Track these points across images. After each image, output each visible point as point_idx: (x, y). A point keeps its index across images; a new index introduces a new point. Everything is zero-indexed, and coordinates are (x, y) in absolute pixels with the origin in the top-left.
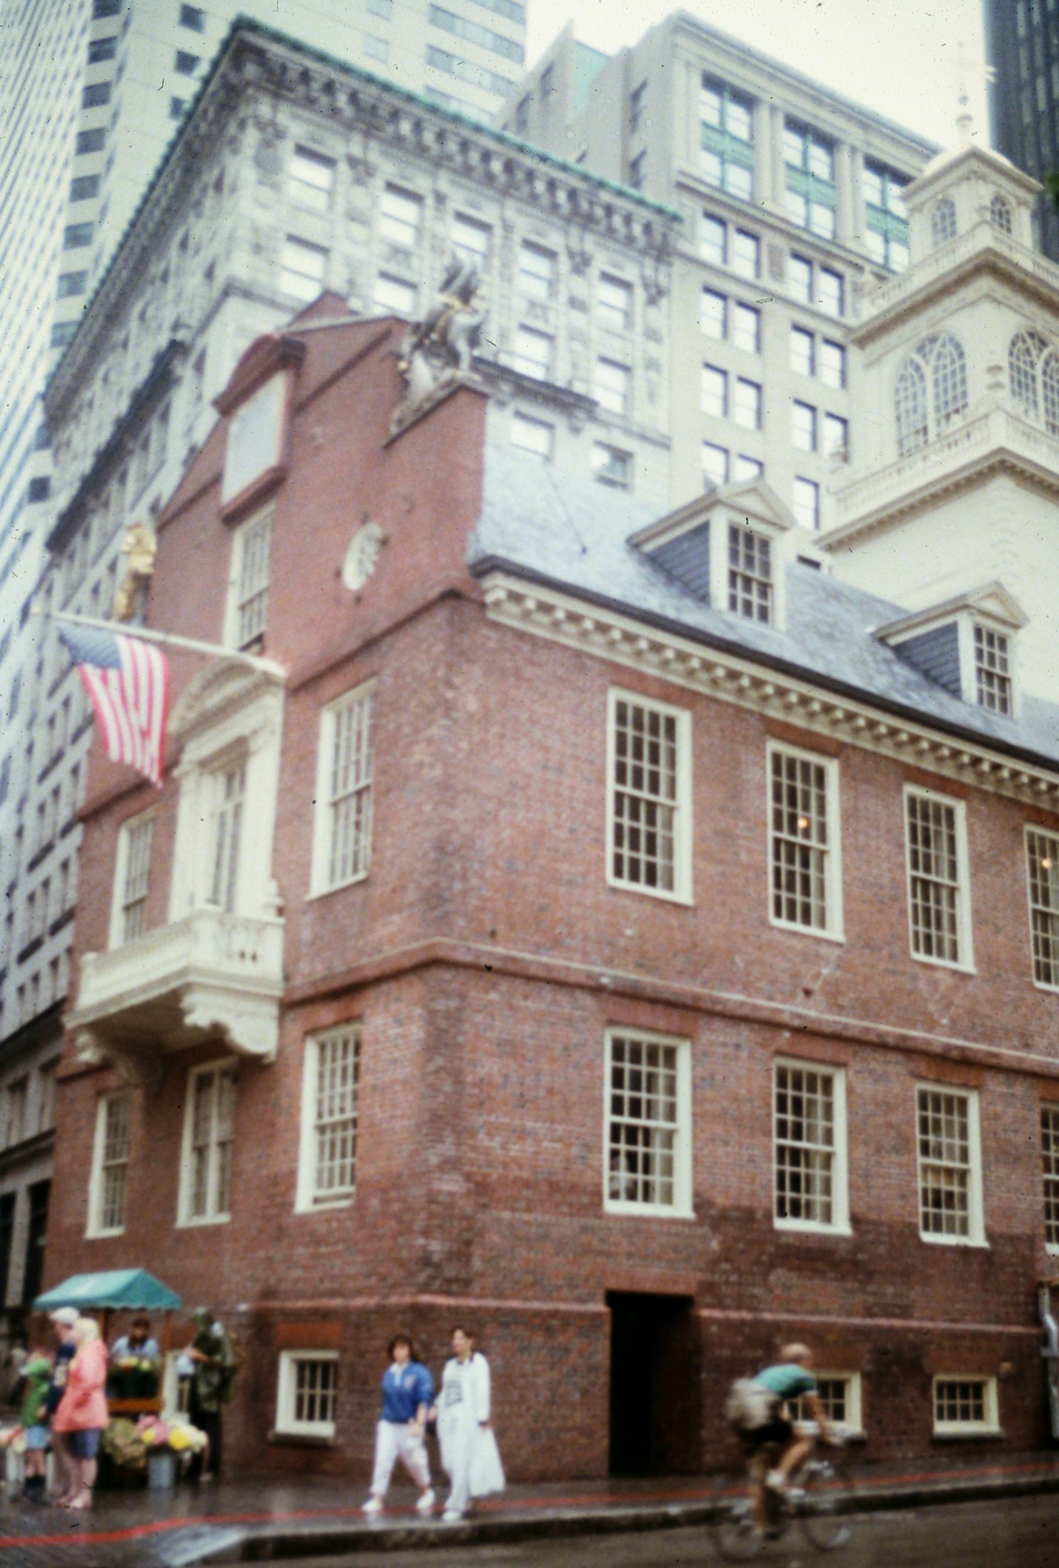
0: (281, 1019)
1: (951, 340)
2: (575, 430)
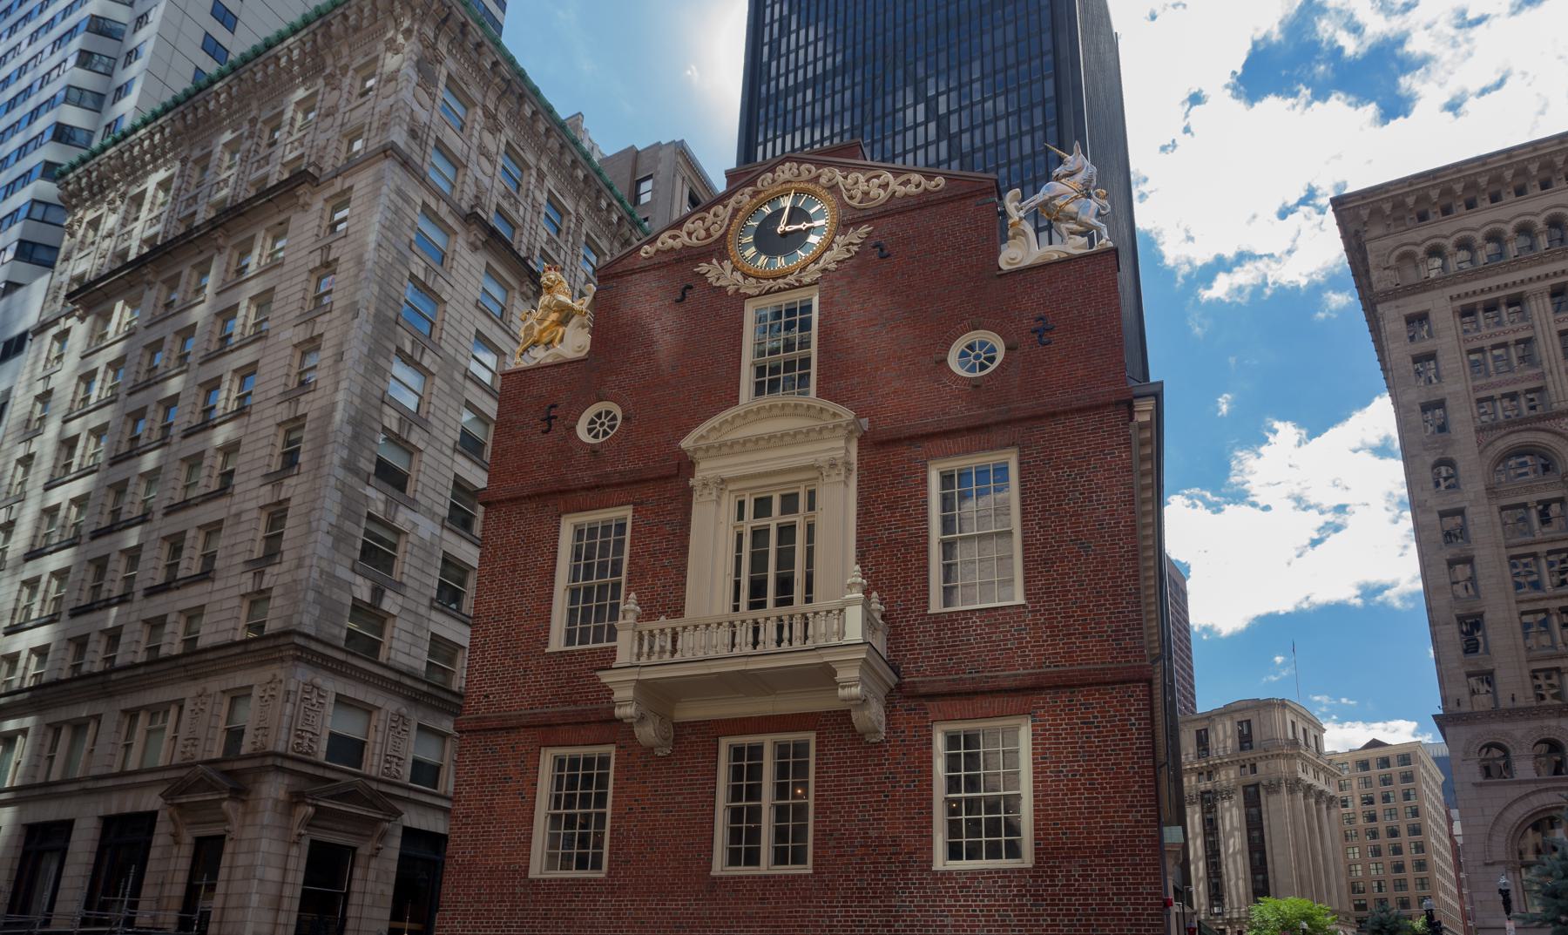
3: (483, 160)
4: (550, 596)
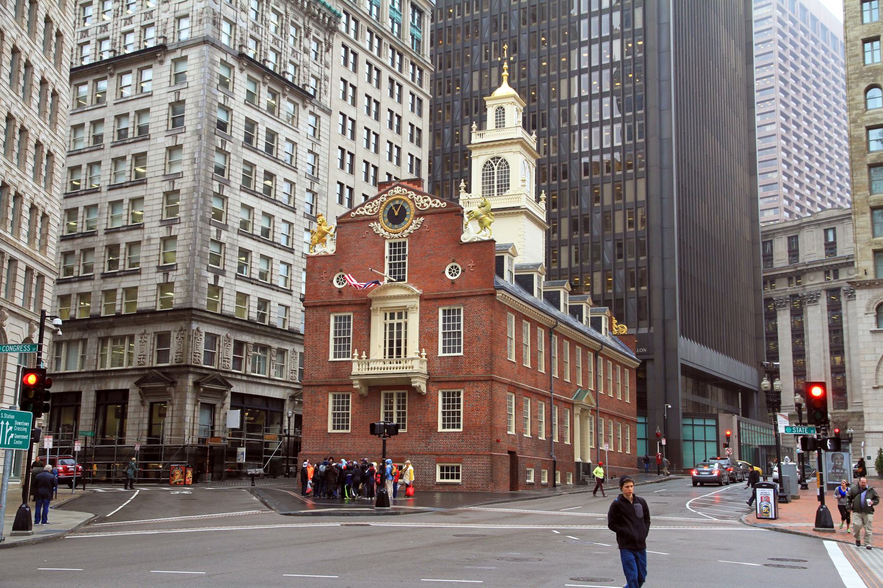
0: (427, 385)
1: (505, 160)
2: (305, 107)
3: (243, 13)
4: (329, 341)
